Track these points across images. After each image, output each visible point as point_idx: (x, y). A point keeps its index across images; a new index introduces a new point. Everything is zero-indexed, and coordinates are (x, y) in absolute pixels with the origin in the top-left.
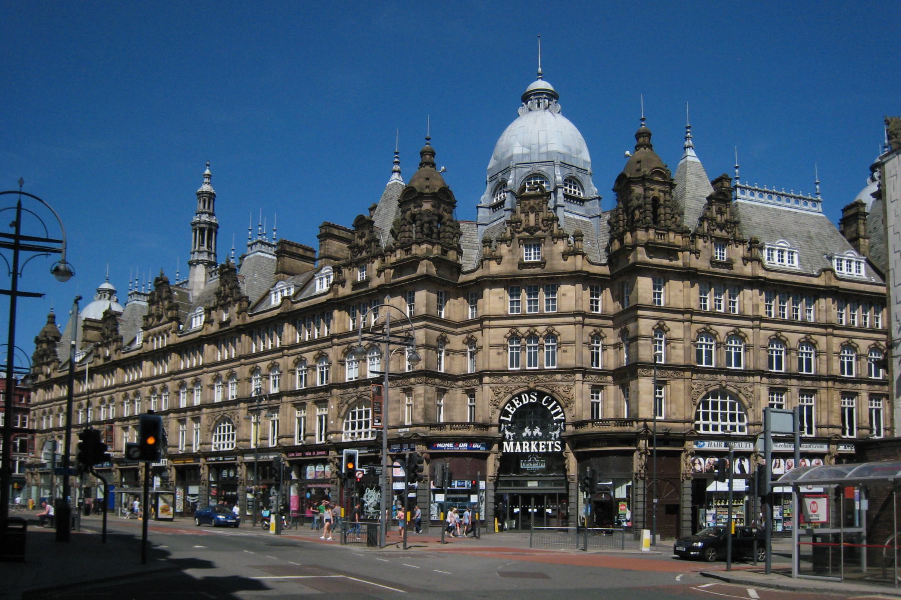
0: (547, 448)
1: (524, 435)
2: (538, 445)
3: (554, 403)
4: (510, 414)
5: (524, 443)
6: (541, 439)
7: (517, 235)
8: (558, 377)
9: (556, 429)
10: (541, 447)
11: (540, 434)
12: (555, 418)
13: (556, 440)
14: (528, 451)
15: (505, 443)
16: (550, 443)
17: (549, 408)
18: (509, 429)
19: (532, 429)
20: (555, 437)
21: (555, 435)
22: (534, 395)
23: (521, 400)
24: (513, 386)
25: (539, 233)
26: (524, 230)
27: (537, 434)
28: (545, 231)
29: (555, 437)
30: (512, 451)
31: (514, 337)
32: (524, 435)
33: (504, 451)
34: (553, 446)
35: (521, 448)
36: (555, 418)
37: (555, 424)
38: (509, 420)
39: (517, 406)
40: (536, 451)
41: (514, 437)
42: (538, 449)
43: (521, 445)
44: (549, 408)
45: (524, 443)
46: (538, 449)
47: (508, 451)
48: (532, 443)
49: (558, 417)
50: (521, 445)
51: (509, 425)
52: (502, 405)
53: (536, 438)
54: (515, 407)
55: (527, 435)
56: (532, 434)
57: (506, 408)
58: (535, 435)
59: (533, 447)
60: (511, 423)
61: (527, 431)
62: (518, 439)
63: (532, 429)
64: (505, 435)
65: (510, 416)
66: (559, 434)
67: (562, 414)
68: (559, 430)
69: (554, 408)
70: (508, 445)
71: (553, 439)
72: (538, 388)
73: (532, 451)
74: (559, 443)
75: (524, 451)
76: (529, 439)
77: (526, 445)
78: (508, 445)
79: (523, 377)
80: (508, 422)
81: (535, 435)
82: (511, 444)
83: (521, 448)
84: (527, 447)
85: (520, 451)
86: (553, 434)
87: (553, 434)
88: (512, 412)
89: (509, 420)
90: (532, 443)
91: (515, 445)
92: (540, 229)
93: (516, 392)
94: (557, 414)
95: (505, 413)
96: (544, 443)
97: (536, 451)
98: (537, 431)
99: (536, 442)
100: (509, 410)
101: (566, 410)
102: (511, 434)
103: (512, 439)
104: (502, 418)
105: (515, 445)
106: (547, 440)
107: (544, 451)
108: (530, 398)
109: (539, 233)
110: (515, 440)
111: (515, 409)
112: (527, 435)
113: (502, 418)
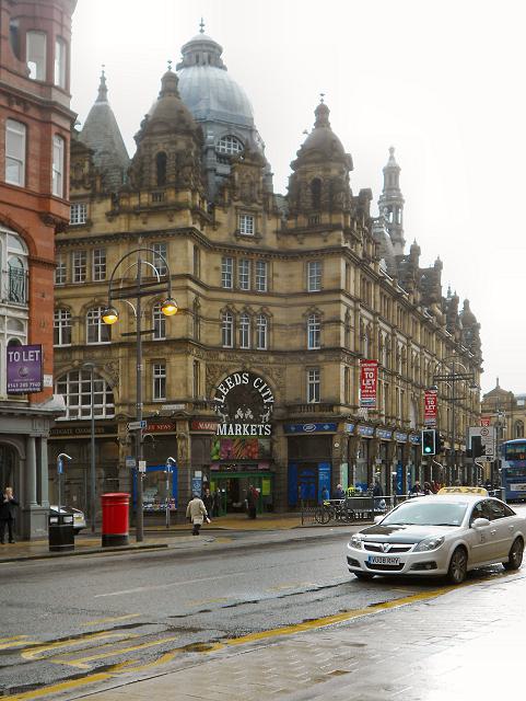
0: (258, 430)
1: (237, 417)
2: (249, 429)
7: (235, 204)
8: (271, 359)
9: (266, 411)
12: (265, 401)
16: (260, 426)
17: (260, 390)
23: (233, 380)
24: (226, 364)
25: (255, 205)
26: (241, 199)
28: (260, 204)
31: (229, 311)
34: (264, 430)
36: (265, 401)
43: (234, 427)
44: (260, 390)
49: (268, 400)
50: (234, 427)
61: (239, 412)
62: (232, 421)
63: (244, 412)
68: (268, 414)
69: (264, 391)
72: (254, 370)
76: (241, 421)
79: (239, 357)
82: (225, 426)
91: (228, 427)
92: (255, 201)
93: (231, 372)
94: (268, 396)
95: (219, 394)
101: (277, 393)
105: (228, 427)
108: (242, 379)
109: (255, 205)
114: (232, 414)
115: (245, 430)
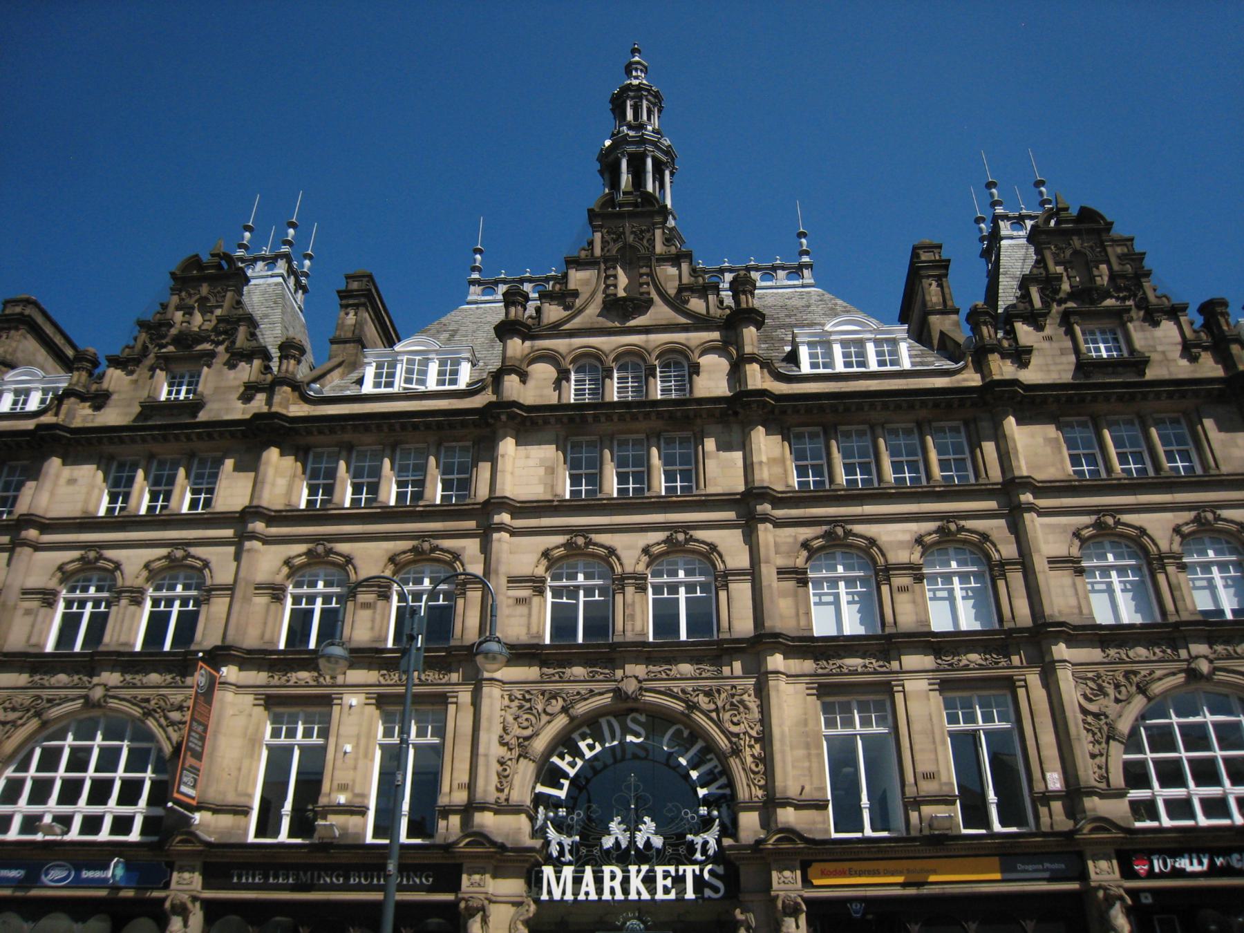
0: (679, 880)
1: (608, 842)
2: (649, 881)
3: (700, 744)
4: (566, 776)
5: (607, 870)
6: (661, 857)
9: (706, 824)
10: (660, 883)
11: (658, 842)
13: (708, 860)
14: (619, 896)
15: (548, 871)
16: (689, 871)
18: (560, 827)
19: (632, 827)
20: (704, 851)
21: (705, 843)
22: (635, 721)
27: (648, 843)
29: (704, 851)
30: (569, 896)
32: (608, 842)
33: (545, 897)
34: (698, 880)
35: (600, 891)
37: (703, 810)
38: (562, 794)
39: (588, 754)
40: (646, 896)
41: (574, 849)
42: (652, 891)
45: (607, 870)
46: (652, 891)
47: (557, 895)
48: (633, 869)
51: (562, 812)
52: (539, 745)
53: (645, 855)
54: (582, 755)
55: (617, 842)
56: (632, 840)
57: (555, 759)
58: (640, 845)
59: (636, 883)
60: (572, 802)
61: (616, 833)
64: (547, 843)
65: (566, 783)
66: (719, 842)
67: (723, 780)
70: (558, 873)
71: (698, 856)
73: (633, 896)
74: (720, 870)
75: (607, 896)
76: (622, 856)
77: (613, 878)
78: (558, 873)
80: (553, 803)
81: (640, 845)
82: (568, 872)
83: (600, 891)
84: (617, 884)
85: (593, 896)
86: (699, 840)
87: (699, 840)
88: (572, 772)
89: (562, 794)
90: (633, 869)
95: (552, 776)
96: (672, 869)
97: (646, 896)
98: (648, 832)
99: (645, 868)
100: (563, 765)
102: (567, 841)
103: (568, 857)
104: (540, 789)
106: (678, 863)
107: (672, 896)
110: (579, 864)
111: (580, 763)
112: (617, 842)
113: (540, 789)
114: (591, 832)
115: (636, 883)
